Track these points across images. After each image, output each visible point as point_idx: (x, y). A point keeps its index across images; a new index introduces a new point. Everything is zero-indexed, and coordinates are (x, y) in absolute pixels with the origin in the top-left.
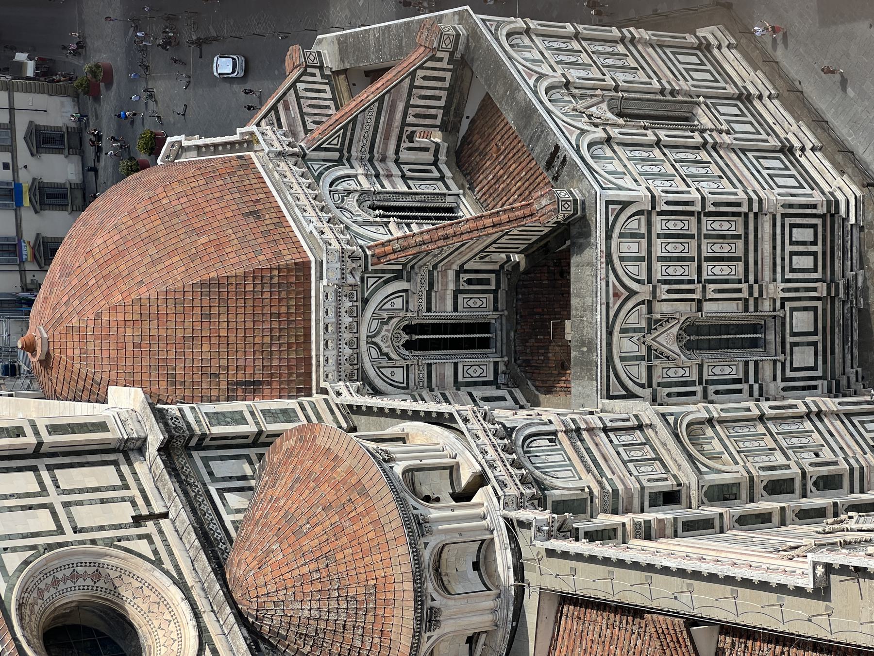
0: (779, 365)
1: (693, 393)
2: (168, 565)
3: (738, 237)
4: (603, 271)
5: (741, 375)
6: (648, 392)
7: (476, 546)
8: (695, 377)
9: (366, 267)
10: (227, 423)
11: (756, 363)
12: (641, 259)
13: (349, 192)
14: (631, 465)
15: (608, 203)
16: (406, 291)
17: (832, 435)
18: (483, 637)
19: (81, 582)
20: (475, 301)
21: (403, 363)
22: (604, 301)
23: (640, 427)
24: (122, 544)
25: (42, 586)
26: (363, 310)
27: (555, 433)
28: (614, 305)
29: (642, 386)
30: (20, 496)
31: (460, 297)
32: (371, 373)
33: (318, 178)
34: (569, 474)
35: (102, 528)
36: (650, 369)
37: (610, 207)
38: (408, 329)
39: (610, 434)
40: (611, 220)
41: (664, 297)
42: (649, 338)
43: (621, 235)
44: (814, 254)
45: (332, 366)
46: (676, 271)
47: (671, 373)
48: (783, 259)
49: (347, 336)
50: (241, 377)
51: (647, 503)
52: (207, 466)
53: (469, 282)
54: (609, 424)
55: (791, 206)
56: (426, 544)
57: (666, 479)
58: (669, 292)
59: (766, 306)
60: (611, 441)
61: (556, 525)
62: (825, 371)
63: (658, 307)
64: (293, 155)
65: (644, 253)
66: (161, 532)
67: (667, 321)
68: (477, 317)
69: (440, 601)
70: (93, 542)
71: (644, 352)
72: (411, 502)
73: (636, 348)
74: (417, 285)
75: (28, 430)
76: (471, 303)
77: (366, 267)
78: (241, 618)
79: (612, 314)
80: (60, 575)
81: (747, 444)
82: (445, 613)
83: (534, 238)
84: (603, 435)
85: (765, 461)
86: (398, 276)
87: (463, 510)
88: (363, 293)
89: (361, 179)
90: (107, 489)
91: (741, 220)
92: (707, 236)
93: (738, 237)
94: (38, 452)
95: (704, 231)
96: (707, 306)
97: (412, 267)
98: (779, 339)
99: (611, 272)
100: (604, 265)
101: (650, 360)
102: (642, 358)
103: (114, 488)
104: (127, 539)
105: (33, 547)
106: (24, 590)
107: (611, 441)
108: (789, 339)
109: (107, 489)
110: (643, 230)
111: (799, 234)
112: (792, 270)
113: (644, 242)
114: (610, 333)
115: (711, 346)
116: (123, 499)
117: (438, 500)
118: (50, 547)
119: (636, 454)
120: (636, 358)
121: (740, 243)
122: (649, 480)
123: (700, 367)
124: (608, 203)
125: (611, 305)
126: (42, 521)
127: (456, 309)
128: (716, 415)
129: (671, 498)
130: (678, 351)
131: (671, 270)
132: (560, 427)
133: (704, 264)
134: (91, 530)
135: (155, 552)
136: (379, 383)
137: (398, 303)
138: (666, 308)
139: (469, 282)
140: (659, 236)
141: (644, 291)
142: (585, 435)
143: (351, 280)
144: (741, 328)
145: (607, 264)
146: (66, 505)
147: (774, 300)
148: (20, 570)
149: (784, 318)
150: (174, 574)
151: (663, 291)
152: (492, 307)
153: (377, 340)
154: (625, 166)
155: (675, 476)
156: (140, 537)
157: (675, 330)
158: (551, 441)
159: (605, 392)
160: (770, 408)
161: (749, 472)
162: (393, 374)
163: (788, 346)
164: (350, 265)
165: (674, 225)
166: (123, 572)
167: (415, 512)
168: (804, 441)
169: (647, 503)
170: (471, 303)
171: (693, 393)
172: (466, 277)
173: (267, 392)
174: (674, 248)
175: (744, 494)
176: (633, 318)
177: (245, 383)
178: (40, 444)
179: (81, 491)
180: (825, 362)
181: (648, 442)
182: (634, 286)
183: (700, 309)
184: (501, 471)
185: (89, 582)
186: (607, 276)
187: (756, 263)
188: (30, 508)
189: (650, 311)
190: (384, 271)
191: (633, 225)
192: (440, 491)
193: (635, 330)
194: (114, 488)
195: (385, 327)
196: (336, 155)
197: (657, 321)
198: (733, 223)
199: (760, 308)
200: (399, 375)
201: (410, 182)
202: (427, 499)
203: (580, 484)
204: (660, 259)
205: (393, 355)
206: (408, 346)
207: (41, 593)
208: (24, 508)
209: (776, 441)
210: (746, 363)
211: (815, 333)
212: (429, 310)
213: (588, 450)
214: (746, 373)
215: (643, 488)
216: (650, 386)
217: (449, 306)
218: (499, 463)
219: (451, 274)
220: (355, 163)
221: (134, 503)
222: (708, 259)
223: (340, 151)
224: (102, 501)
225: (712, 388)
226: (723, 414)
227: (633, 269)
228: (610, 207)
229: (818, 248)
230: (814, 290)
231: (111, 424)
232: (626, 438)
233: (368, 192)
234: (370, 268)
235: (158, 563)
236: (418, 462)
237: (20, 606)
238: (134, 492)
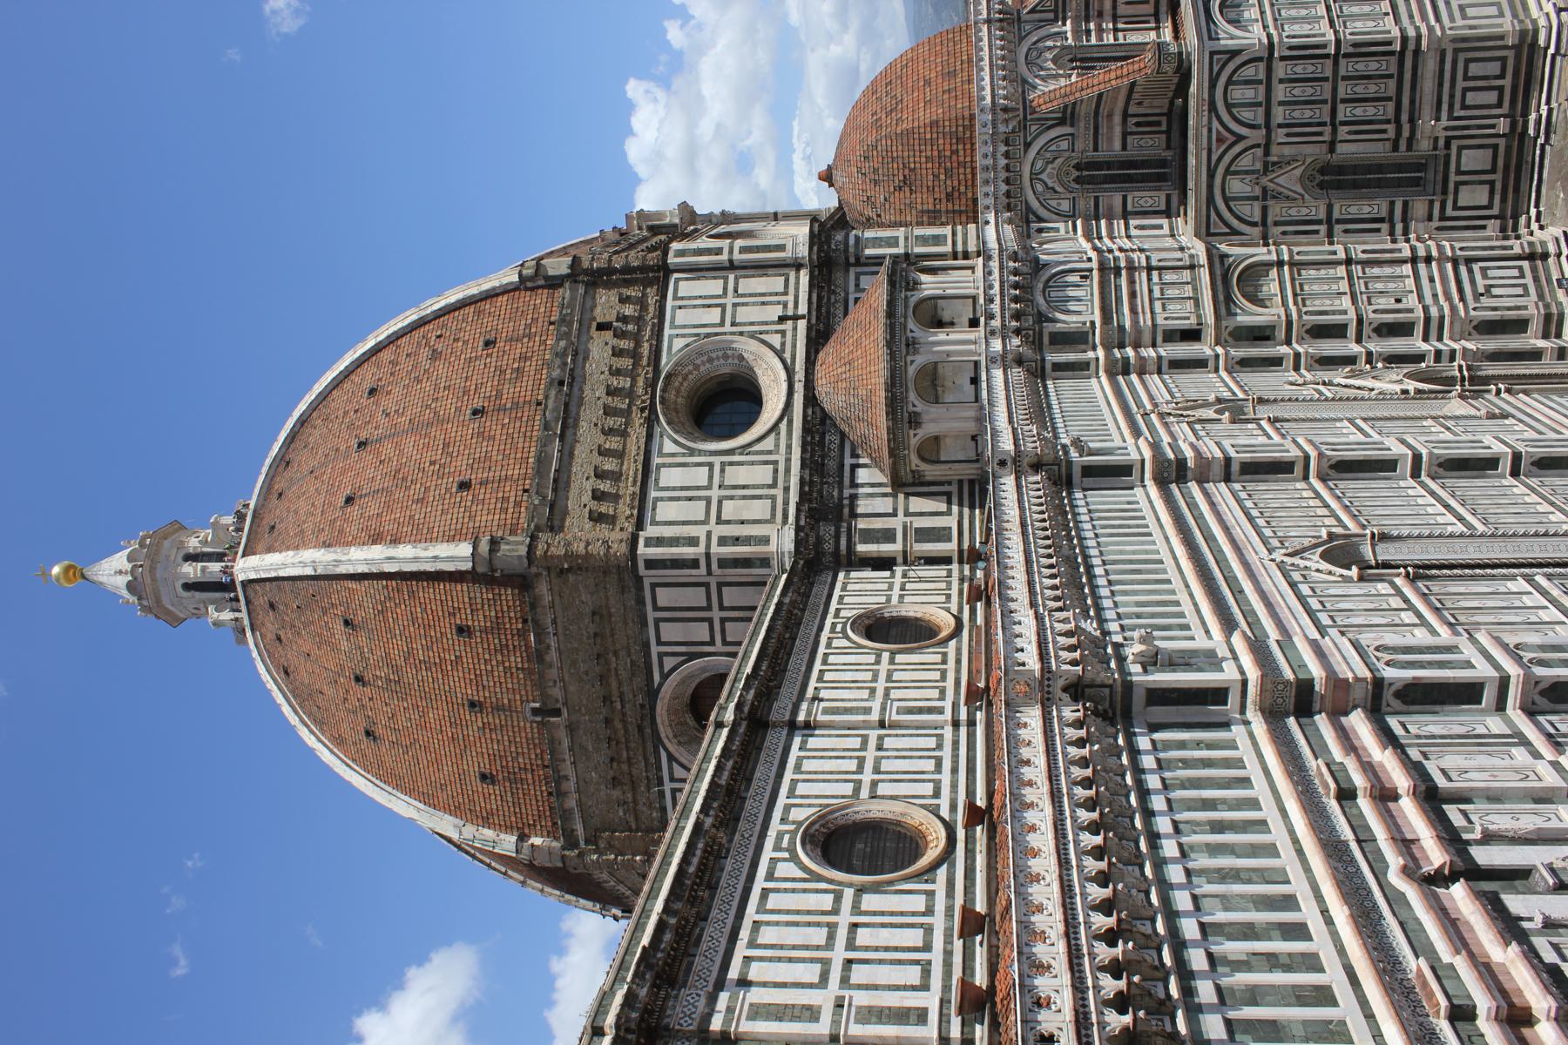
0: (1437, 206)
1: (1317, 232)
2: (787, 356)
3: (1390, 76)
4: (1205, 119)
5: (1384, 214)
6: (1257, 231)
7: (972, 365)
8: (1322, 215)
9: (1025, 116)
10: (880, 246)
11: (1405, 204)
12: (1259, 104)
13: (1050, 48)
14: (1158, 305)
15: (1212, 54)
16: (1072, 135)
17: (1432, 280)
18: (979, 438)
19: (730, 361)
20: (1148, 141)
21: (1068, 196)
22: (1205, 145)
23: (1192, 267)
24: (763, 337)
25: (698, 362)
26: (1025, 152)
27: (1091, 270)
28: (1217, 149)
29: (1254, 224)
30: (705, 297)
31: (1130, 139)
32: (1035, 204)
33: (1021, 39)
34: (1084, 308)
35: (752, 324)
36: (1264, 210)
37: (1215, 57)
38: (1077, 167)
39: (1155, 274)
40: (1216, 69)
41: (1280, 140)
42: (1264, 181)
43: (1229, 82)
44: (1501, 89)
45: (990, 201)
46: (1306, 114)
47: (1293, 212)
48: (1452, 96)
49: (1004, 175)
50: (925, 207)
51: (1159, 339)
52: (857, 279)
53: (1138, 124)
54: (1154, 263)
55: (1464, 39)
56: (912, 362)
57: (1188, 318)
58: (1288, 135)
59: (1424, 145)
60: (1149, 280)
61: (1010, 357)
62: (1503, 210)
63: (1274, 149)
64: (1000, 20)
65: (1261, 98)
66: (795, 329)
67: (1289, 163)
68: (1149, 155)
69: (920, 407)
70: (741, 334)
71: (1258, 191)
72: (911, 324)
73: (1249, 189)
74: (1083, 128)
75: (726, 251)
76: (1141, 143)
77: (1025, 116)
78: (811, 399)
79: (1214, 158)
80: (714, 355)
81: (1315, 287)
82: (925, 417)
83: (1173, 87)
84: (1144, 275)
85: (1326, 304)
86: (1061, 122)
87: (972, 335)
88: (1025, 137)
89: (1069, 35)
90: (771, 294)
91: (1394, 60)
92: (1344, 78)
93: (1390, 76)
94: (732, 266)
95: (1342, 72)
96: (1341, 148)
97: (1073, 113)
98: (1440, 177)
99: (1214, 119)
100: (1206, 113)
101: (1265, 199)
102: (1256, 198)
103: (777, 294)
104: (767, 332)
105: (697, 335)
106: (677, 364)
107: (1149, 280)
108: (1453, 178)
109: (771, 294)
110: (1262, 76)
111: (1475, 69)
112: (1464, 107)
113: (1262, 88)
114: (1211, 175)
115: (1356, 185)
116: (779, 303)
117: (952, 324)
118: (708, 335)
119: (1170, 292)
120: (1249, 198)
121: (1392, 83)
122: (1166, 319)
123: (1330, 208)
124: (1212, 54)
125: (1214, 149)
126: (714, 316)
127: (1124, 147)
128: (1286, 258)
129: (1192, 335)
130: (1301, 191)
131: (1296, 114)
132: (1095, 265)
133: (1341, 107)
134: (744, 324)
135: (783, 344)
136: (1042, 212)
137: (1064, 145)
138: (1287, 150)
139: (1138, 124)
140: (1281, 81)
141: (1258, 136)
142: (1124, 272)
143: (1002, 128)
144: (1400, 167)
145: (1210, 112)
146: (735, 305)
147: (1436, 139)
148: (680, 351)
149: (1448, 157)
150: (789, 361)
151: (1280, 135)
152: (1164, 146)
153: (1044, 176)
154: (1262, 13)
155: (1199, 316)
156: (777, 332)
157: (1298, 172)
158: (1082, 277)
159: (1204, 230)
160: (1364, 252)
161: (1288, 316)
162: (1059, 204)
163: (1451, 186)
164: (1002, 116)
165: (1301, 69)
166: (758, 357)
167: (910, 335)
168: (1391, 286)
169: (1159, 339)
170: (1141, 143)
171: (1317, 232)
172: (1135, 120)
173: (944, 220)
174: (1299, 91)
175: (1281, 334)
176: (1245, 162)
177: (928, 211)
178: (731, 261)
179: (751, 295)
180: (1504, 200)
181: (1194, 283)
182: (1243, 131)
183: (1332, 150)
184: (996, 307)
185: (736, 361)
186: (1210, 122)
187: (1412, 102)
188: (709, 306)
189: (1267, 153)
190: (1047, 119)
191: (1249, 72)
192: (960, 316)
193: (1247, 172)
194: (777, 294)
195: (1050, 166)
196: (1051, 16)
197: (1274, 164)
198: (1384, 63)
199: (1414, 148)
200: (1065, 206)
201: (1120, 35)
202: (940, 324)
203: (1087, 318)
204: (1281, 103)
205: (1058, 189)
206: (1077, 180)
207: (697, 367)
208: (704, 306)
209: (1351, 285)
210: (1392, 203)
211: (1493, 170)
212: (1096, 149)
213: (1118, 288)
214: (1391, 212)
215: (1154, 326)
216: (1264, 223)
217: (1117, 145)
218: (997, 300)
219: (1117, 119)
220: (1069, 22)
221: (785, 305)
222: (1344, 101)
223: (1055, 11)
224: (763, 303)
225: (1338, 228)
226: (1296, 257)
227: (1246, 115)
228: (1215, 57)
229: (1507, 82)
230: (1493, 126)
231: (789, 247)
232: (1169, 277)
233: (1070, 46)
234: (1029, 117)
235: (779, 354)
236: (941, 292)
237: (669, 376)
238: (790, 298)
